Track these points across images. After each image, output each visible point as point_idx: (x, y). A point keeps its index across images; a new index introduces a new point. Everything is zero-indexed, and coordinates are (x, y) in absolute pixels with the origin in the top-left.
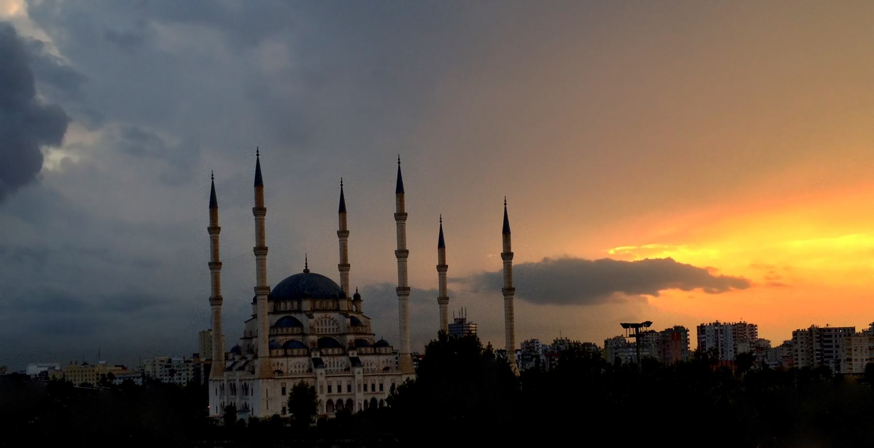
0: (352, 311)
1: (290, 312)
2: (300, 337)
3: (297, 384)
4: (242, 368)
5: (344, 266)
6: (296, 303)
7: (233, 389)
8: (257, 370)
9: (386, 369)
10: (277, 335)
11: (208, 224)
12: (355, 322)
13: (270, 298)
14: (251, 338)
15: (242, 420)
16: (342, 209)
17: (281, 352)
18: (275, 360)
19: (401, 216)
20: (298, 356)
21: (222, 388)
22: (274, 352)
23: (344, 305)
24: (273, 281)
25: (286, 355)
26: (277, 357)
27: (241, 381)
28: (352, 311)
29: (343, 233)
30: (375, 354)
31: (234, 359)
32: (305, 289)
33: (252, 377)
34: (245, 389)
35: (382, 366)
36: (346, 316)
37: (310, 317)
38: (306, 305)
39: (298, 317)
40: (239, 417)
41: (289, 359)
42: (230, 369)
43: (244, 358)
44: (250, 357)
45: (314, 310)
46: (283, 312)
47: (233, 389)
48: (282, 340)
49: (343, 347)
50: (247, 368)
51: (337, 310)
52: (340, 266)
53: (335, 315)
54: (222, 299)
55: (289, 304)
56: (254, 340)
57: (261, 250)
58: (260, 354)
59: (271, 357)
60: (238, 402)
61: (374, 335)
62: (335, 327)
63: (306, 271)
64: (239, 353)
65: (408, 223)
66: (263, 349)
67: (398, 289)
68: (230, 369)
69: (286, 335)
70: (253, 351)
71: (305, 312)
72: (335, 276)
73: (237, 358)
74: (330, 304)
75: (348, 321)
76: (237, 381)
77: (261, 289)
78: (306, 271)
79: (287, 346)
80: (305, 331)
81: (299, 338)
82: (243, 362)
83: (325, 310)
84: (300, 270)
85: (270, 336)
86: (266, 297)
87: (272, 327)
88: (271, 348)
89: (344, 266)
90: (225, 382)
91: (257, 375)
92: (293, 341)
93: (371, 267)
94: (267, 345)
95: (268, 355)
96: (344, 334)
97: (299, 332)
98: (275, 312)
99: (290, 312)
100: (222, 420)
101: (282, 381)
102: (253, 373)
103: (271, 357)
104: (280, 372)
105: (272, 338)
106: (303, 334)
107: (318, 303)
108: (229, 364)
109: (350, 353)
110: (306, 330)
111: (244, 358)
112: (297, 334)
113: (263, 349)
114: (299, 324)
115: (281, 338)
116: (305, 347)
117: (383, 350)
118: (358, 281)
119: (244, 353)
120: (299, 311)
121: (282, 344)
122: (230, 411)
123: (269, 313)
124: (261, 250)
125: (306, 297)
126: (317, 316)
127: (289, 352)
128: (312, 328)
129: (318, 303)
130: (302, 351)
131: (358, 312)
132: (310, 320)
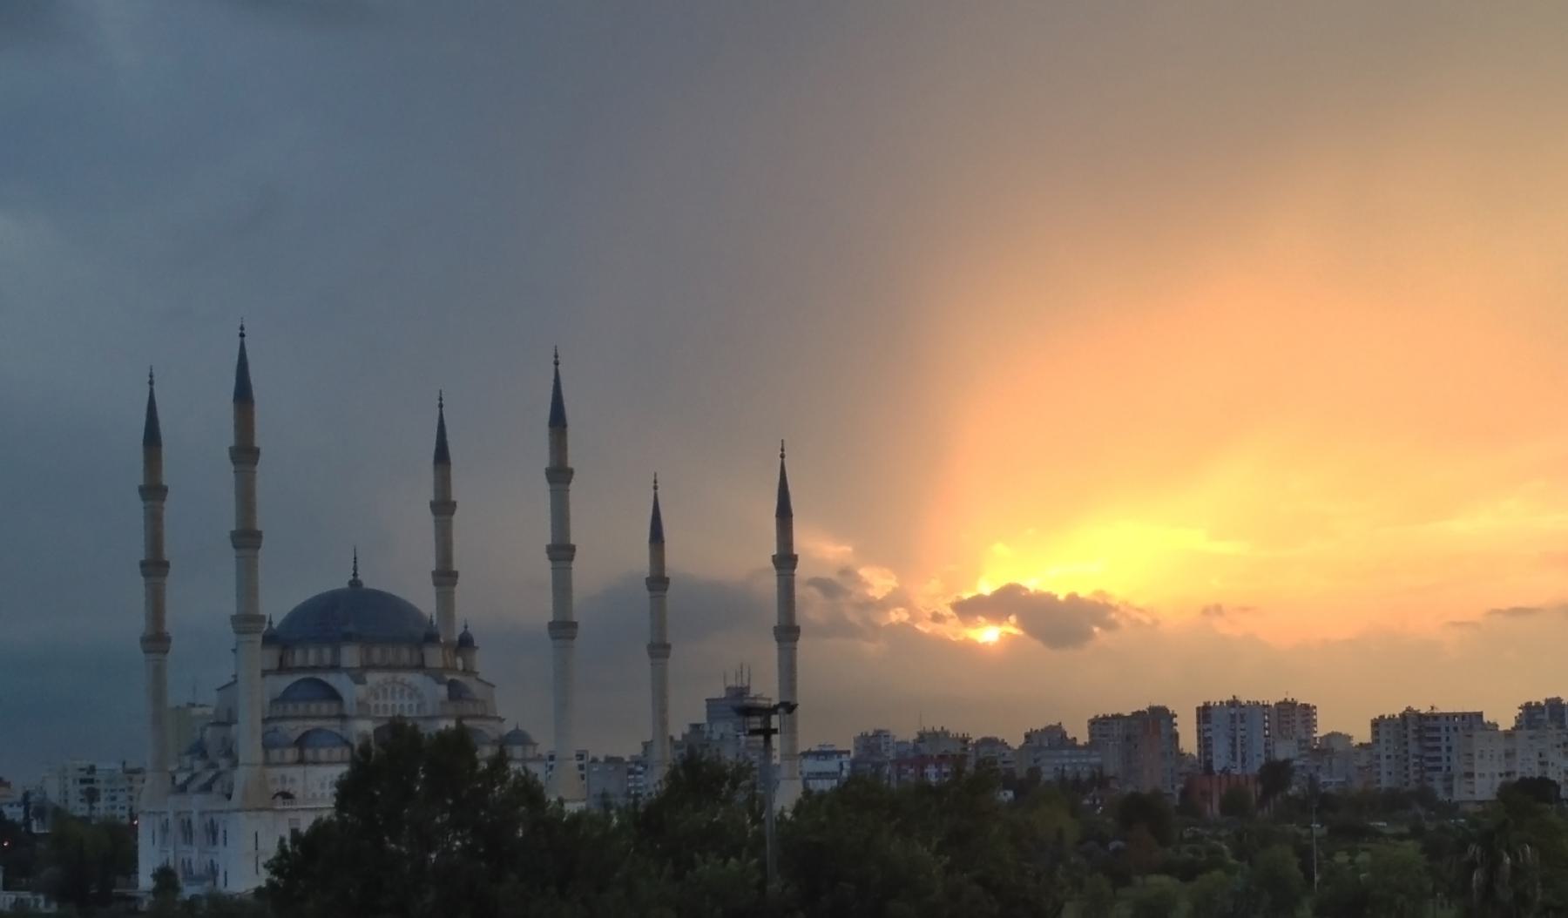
0: (454, 669)
1: (315, 668)
2: (337, 723)
3: (304, 828)
4: (207, 788)
5: (445, 576)
7: (187, 830)
8: (236, 794)
10: (283, 718)
11: (140, 479)
12: (457, 692)
13: (270, 639)
15: (194, 898)
16: (442, 456)
17: (291, 754)
18: (275, 772)
19: (560, 475)
20: (330, 763)
21: (165, 829)
22: (275, 754)
23: (435, 657)
24: (277, 605)
25: (301, 761)
26: (278, 764)
27: (202, 813)
28: (454, 669)
29: (443, 507)
31: (192, 768)
32: (352, 619)
33: (226, 805)
34: (212, 832)
36: (439, 681)
37: (359, 680)
38: (351, 656)
39: (331, 679)
40: (188, 891)
41: (309, 768)
42: (183, 789)
43: (213, 765)
44: (223, 764)
45: (368, 667)
46: (302, 669)
47: (187, 830)
48: (293, 729)
50: (217, 787)
51: (420, 667)
52: (436, 574)
53: (415, 678)
54: (169, 640)
56: (234, 727)
57: (247, 539)
58: (241, 760)
59: (267, 763)
61: (501, 720)
62: (415, 703)
63: (355, 583)
65: (575, 488)
66: (249, 744)
67: (553, 626)
68: (183, 789)
69: (305, 717)
70: (230, 753)
71: (347, 670)
72: (424, 601)
73: (198, 765)
75: (443, 691)
76: (196, 812)
77: (246, 621)
78: (355, 583)
79: (302, 742)
80: (347, 712)
81: (333, 725)
82: (211, 774)
83: (389, 667)
84: (341, 582)
85: (265, 721)
86: (259, 638)
87: (274, 701)
88: (268, 746)
89: (445, 576)
90: (171, 817)
92: (318, 730)
93: (503, 581)
94: (258, 742)
95: (259, 756)
97: (334, 713)
98: (282, 668)
99: (315, 668)
100: (151, 898)
101: (292, 815)
102: (229, 797)
103: (267, 763)
104: (287, 796)
105: (271, 725)
106: (343, 717)
108: (181, 778)
110: (350, 707)
111: (213, 765)
112: (328, 717)
113: (249, 744)
114: (333, 695)
115: (291, 725)
116: (347, 743)
118: (469, 609)
119: (206, 756)
120: (335, 667)
121: (295, 736)
122: (165, 877)
123: (265, 673)
125: (348, 638)
126: (374, 678)
127: (309, 753)
128: (359, 704)
129: (376, 654)
130: (337, 753)
131: (468, 671)
132: (360, 691)
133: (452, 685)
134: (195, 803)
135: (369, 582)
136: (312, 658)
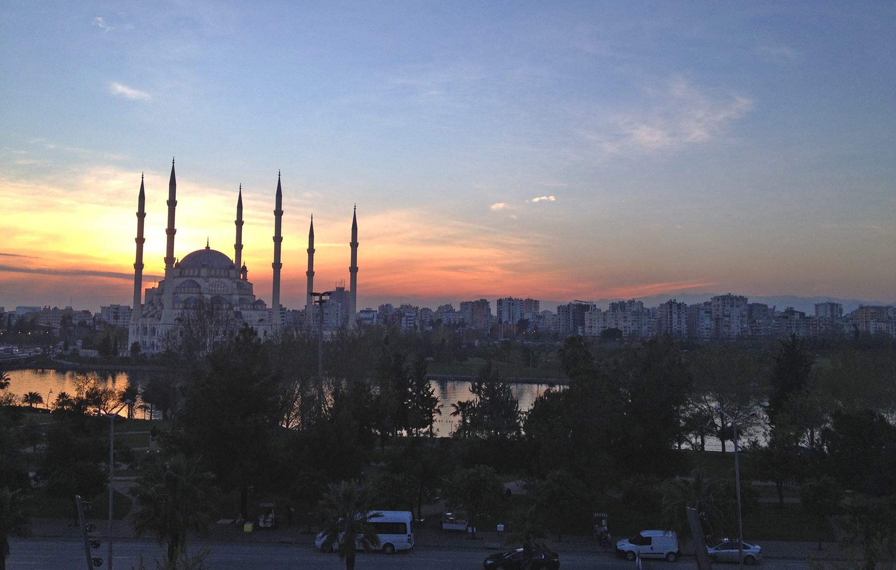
4: (152, 316)
5: (239, 247)
6: (196, 271)
9: (261, 320)
14: (161, 294)
21: (138, 330)
23: (233, 273)
24: (180, 254)
30: (254, 309)
35: (258, 318)
38: (204, 272)
39: (197, 280)
40: (143, 351)
42: (144, 316)
44: (159, 308)
45: (208, 277)
48: (183, 297)
49: (230, 304)
51: (228, 277)
53: (226, 281)
55: (192, 271)
58: (165, 306)
60: (147, 339)
63: (208, 248)
64: (153, 305)
68: (144, 316)
70: (161, 305)
72: (231, 255)
74: (223, 272)
75: (235, 285)
78: (208, 248)
83: (216, 277)
88: (173, 303)
89: (239, 247)
91: (162, 321)
96: (231, 294)
98: (181, 276)
103: (173, 308)
106: (201, 293)
107: (213, 271)
108: (144, 313)
109: (235, 309)
114: (199, 286)
115: (181, 296)
117: (259, 307)
120: (199, 276)
122: (136, 346)
124: (171, 232)
125: (203, 266)
126: (211, 280)
133: (238, 283)
134: (148, 322)
135: (212, 247)
136: (191, 274)
